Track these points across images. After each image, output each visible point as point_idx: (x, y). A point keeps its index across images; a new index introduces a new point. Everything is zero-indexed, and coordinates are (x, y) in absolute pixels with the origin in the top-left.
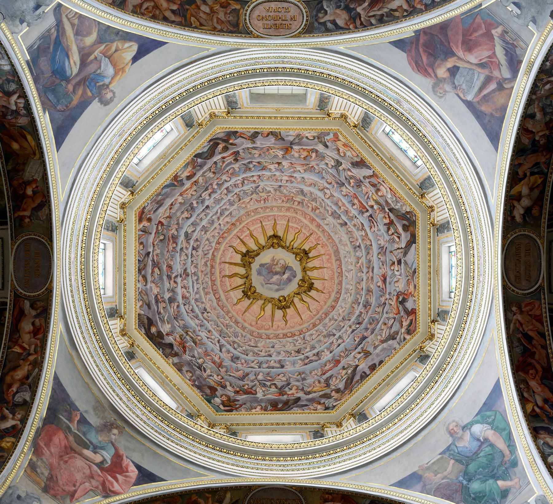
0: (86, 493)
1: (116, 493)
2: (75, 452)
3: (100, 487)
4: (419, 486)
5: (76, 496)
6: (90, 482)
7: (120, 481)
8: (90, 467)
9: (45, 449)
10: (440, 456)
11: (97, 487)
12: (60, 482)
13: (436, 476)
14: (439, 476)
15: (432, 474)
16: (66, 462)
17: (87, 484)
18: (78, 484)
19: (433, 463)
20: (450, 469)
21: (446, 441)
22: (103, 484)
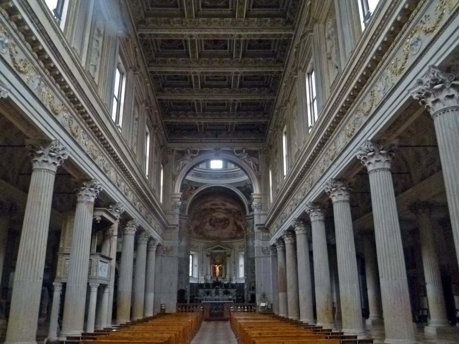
21: (245, 185)
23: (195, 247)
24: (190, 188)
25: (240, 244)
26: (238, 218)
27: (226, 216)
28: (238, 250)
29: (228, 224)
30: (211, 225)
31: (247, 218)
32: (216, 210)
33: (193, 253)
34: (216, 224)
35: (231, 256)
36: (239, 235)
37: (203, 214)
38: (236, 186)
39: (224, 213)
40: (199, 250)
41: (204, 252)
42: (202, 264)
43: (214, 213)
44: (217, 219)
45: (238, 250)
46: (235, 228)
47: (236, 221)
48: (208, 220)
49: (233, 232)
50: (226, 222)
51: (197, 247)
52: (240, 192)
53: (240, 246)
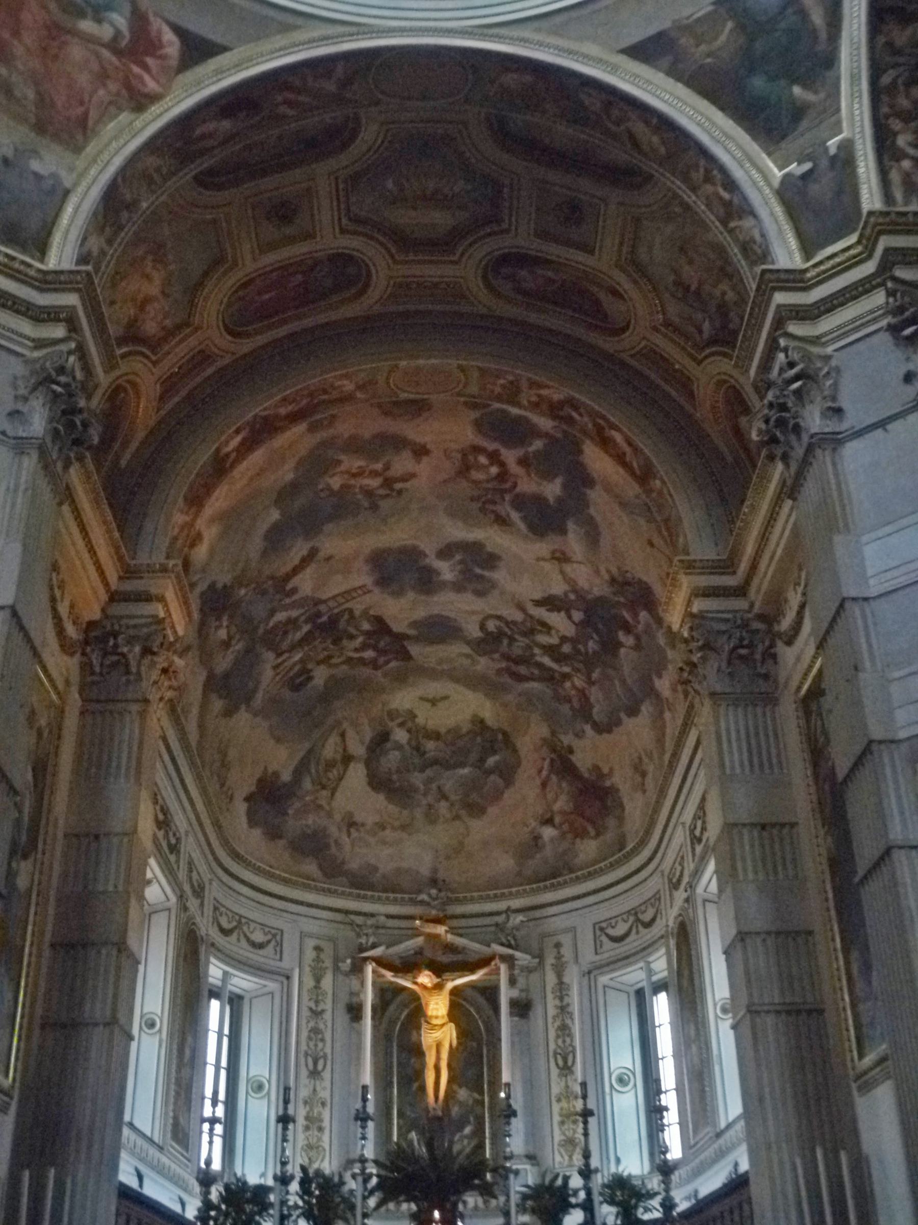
0: (105, 115)
1: (154, 98)
2: (69, 32)
3: (124, 92)
4: (666, 61)
5: (90, 123)
6: (104, 85)
7: (154, 71)
8: (98, 56)
9: (15, 42)
10: (710, 8)
11: (118, 94)
12: (59, 104)
13: (697, 46)
14: (703, 48)
15: (692, 41)
16: (56, 57)
17: (101, 92)
18: (86, 99)
19: (699, 20)
20: (723, 38)
22: (128, 87)
23: (258, 937)
24: (120, 20)
25: (603, 913)
26: (584, 712)
27: (488, 710)
28: (588, 956)
29: (508, 773)
30: (377, 782)
31: (780, 298)
32: (414, 650)
33: (242, 982)
34: (417, 779)
35: (537, 1012)
36: (588, 848)
37: (321, 675)
38: (636, 35)
39: (474, 682)
40: (289, 962)
41: (327, 982)
42: (315, 1074)
43: (401, 679)
44: (420, 734)
45: (588, 956)
46: (562, 804)
47: (567, 739)
48: (358, 749)
49: (548, 832)
50: (491, 761)
51: (276, 938)
52: (681, 90)
53: (600, 929)
